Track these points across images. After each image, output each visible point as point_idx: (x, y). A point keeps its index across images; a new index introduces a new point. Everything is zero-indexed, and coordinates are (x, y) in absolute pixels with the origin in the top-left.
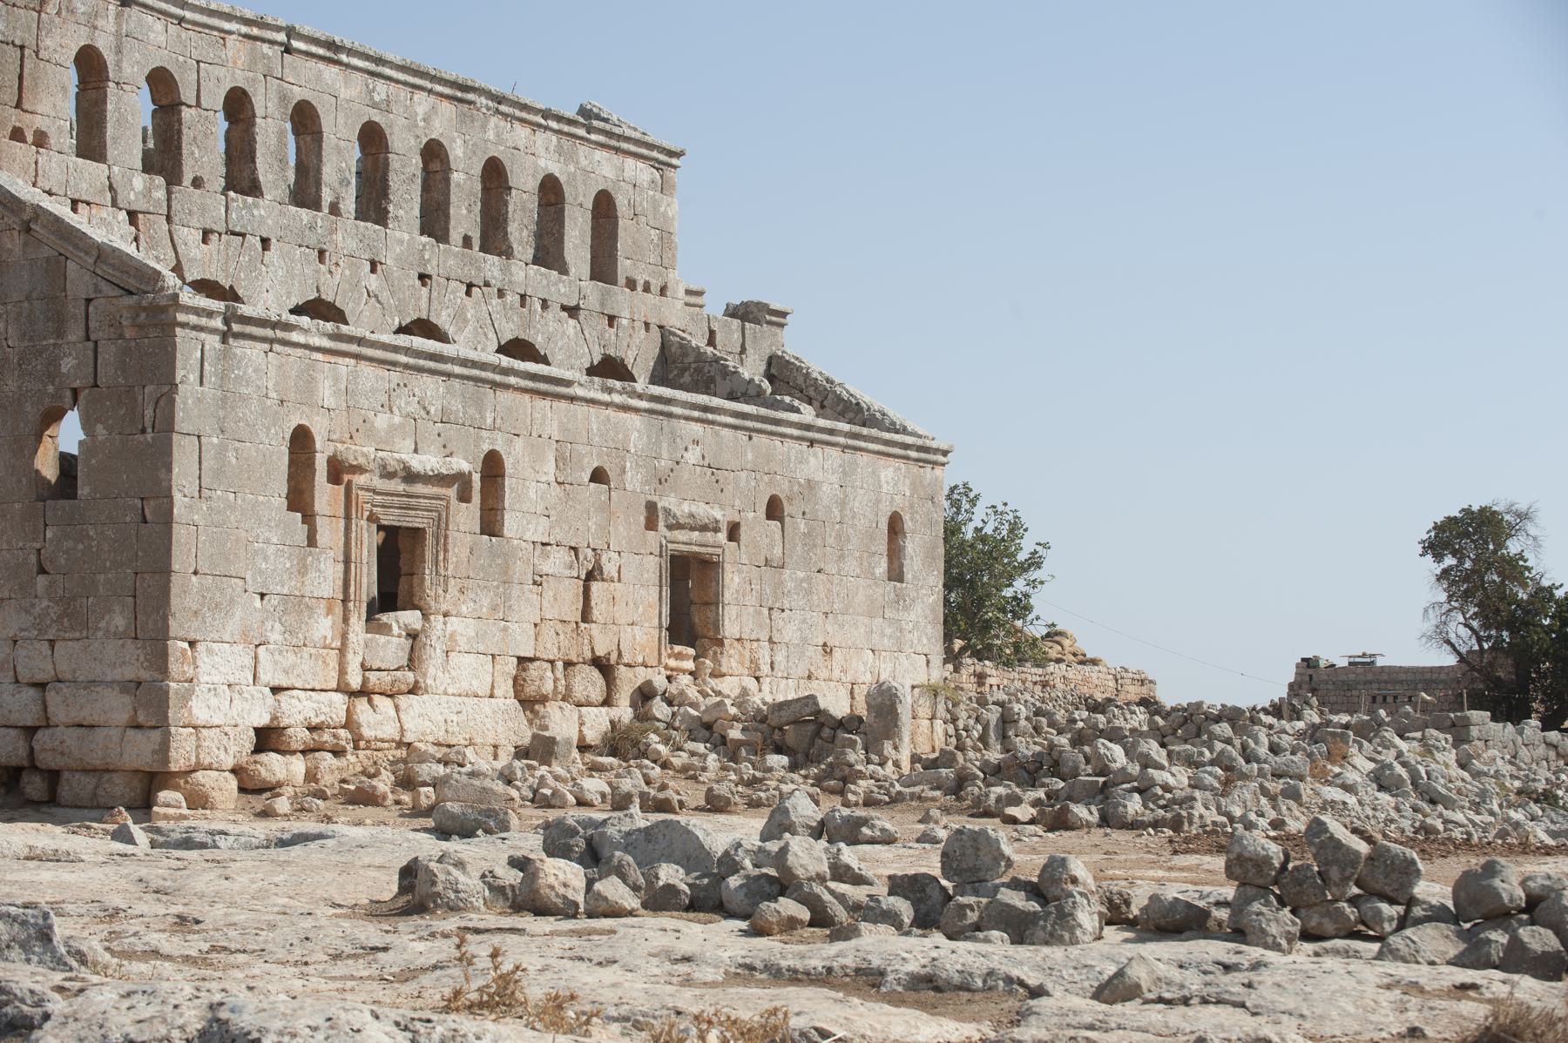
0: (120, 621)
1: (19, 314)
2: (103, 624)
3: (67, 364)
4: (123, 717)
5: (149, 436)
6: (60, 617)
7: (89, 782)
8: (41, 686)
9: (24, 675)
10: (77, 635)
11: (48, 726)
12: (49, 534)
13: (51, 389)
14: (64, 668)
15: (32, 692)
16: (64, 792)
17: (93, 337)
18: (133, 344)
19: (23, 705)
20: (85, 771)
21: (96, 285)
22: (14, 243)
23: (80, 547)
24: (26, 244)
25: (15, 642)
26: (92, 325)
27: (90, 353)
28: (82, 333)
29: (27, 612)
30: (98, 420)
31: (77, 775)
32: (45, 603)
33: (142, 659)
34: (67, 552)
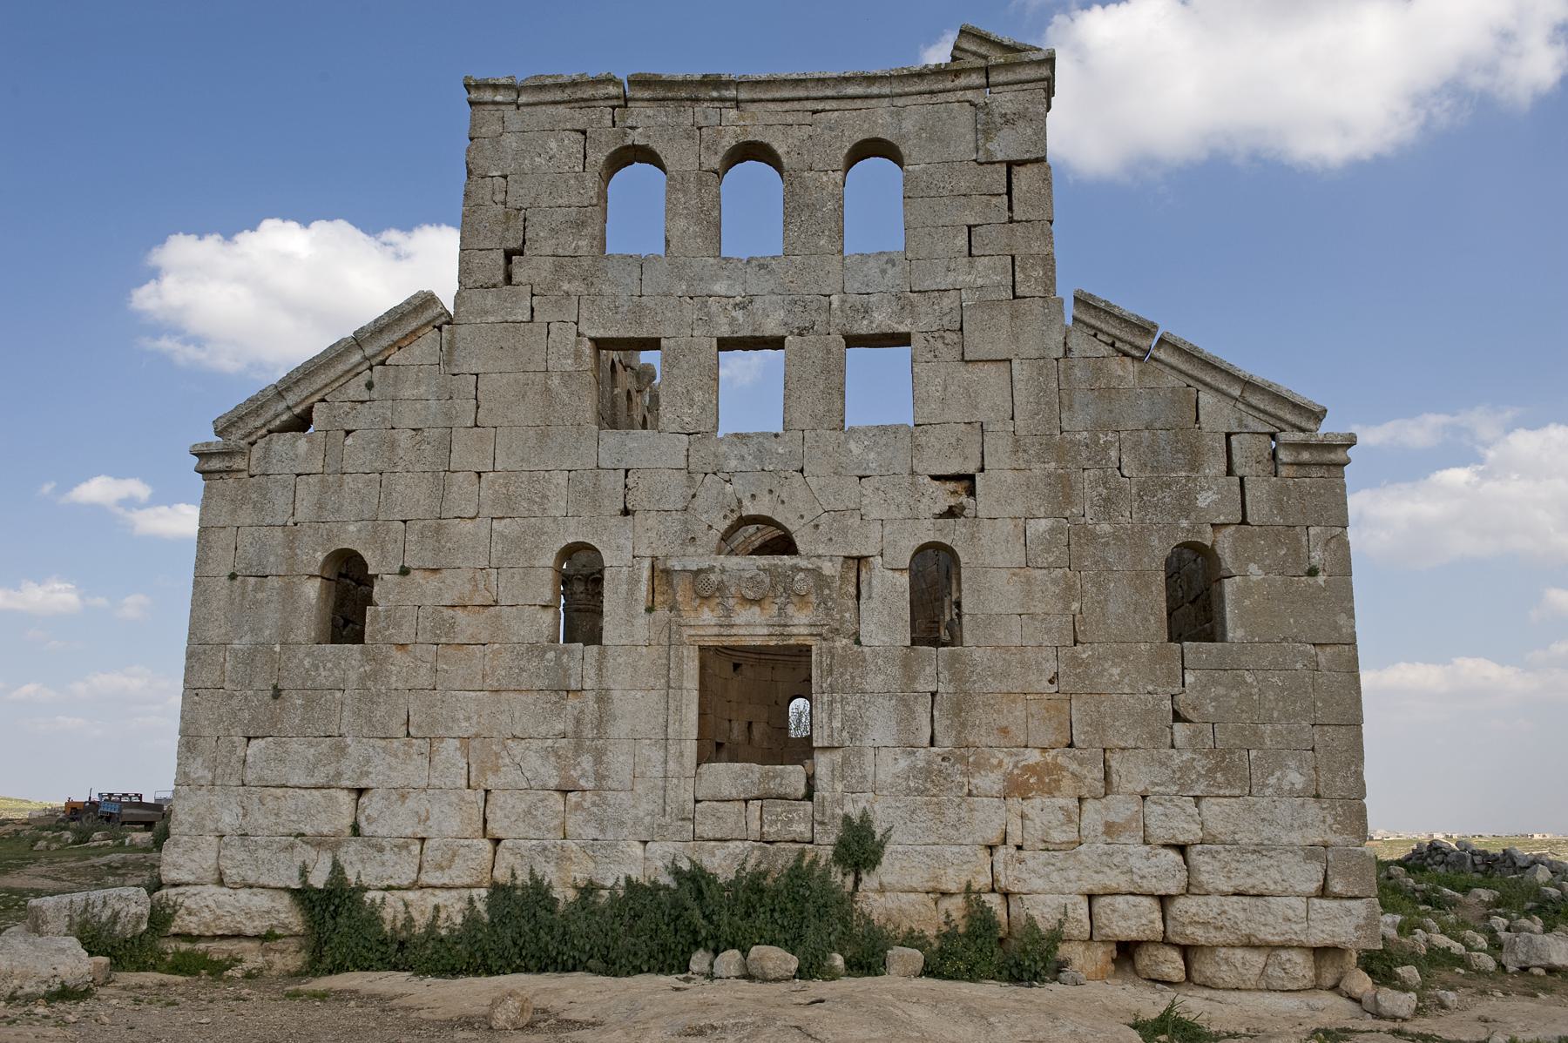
0: (1296, 779)
1: (1137, 444)
2: (1272, 780)
3: (1204, 500)
4: (1313, 887)
5: (1321, 579)
6: (1211, 772)
7: (1257, 959)
8: (1182, 849)
9: (1159, 833)
10: (1237, 792)
11: (1187, 892)
12: (1189, 678)
13: (1184, 523)
14: (1217, 827)
15: (1174, 856)
16: (1206, 968)
17: (1239, 472)
18: (1290, 482)
19: (1164, 871)
20: (1250, 945)
21: (1240, 421)
22: (1124, 371)
23: (1235, 694)
24: (1142, 372)
25: (1144, 797)
26: (1236, 459)
27: (1237, 489)
28: (1224, 468)
29: (1162, 764)
30: (1250, 559)
31: (1239, 953)
32: (1187, 756)
33: (1330, 820)
34: (1215, 699)
